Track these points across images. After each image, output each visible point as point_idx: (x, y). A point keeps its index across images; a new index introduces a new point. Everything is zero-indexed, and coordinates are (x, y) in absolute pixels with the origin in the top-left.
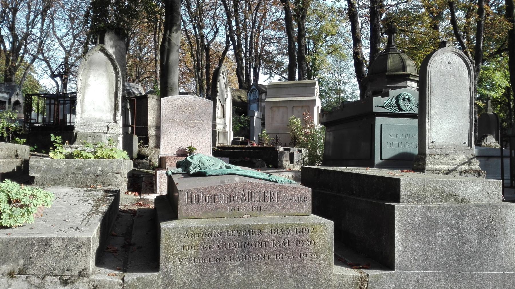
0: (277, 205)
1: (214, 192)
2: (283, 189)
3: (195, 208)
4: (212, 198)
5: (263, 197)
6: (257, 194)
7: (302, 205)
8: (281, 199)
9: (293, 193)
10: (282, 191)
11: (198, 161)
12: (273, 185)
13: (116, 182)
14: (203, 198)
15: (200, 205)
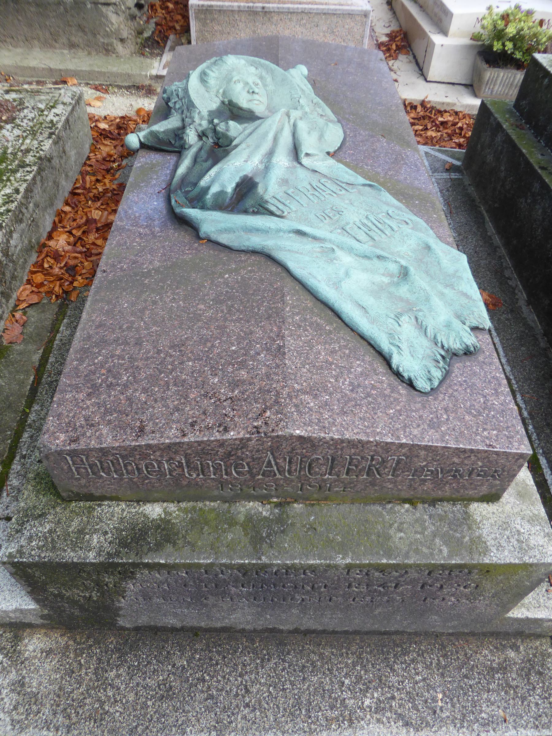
0: (388, 484)
1: (161, 456)
2: (423, 453)
3: (109, 485)
4: (159, 467)
5: (344, 467)
6: (320, 461)
7: (479, 483)
8: (408, 471)
9: (456, 460)
10: (417, 456)
11: (221, 91)
12: (387, 443)
13: (108, 27)
14: (129, 468)
15: (122, 479)
